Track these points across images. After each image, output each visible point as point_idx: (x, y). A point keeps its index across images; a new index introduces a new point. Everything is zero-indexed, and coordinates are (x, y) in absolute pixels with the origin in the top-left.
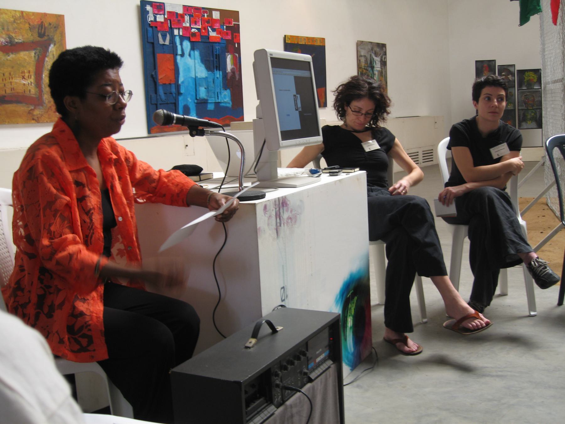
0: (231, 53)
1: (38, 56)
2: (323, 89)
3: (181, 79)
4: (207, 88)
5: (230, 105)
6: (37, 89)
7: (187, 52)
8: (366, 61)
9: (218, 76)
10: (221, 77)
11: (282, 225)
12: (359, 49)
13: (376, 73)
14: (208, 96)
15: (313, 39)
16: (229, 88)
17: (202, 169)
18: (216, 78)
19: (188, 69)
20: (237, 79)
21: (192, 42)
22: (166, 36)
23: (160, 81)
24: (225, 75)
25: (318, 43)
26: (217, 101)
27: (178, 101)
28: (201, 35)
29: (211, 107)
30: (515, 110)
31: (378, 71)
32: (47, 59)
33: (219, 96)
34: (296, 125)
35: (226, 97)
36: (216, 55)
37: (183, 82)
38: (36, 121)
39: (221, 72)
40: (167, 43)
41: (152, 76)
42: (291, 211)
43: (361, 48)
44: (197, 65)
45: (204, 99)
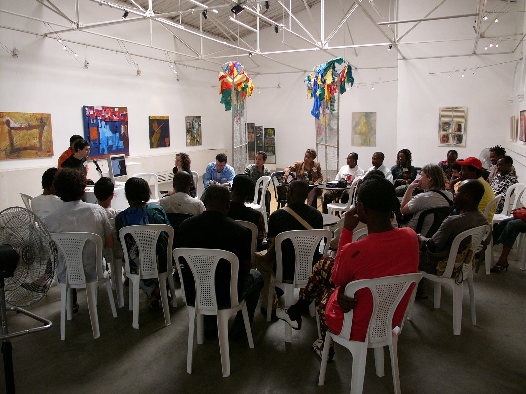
1: (40, 130)
2: (168, 138)
3: (101, 138)
4: (112, 141)
5: (123, 147)
6: (40, 144)
7: (103, 126)
9: (117, 135)
10: (119, 136)
12: (187, 120)
14: (113, 144)
15: (163, 117)
16: (123, 140)
18: (116, 137)
19: (104, 133)
20: (126, 136)
21: (105, 122)
22: (94, 119)
23: (91, 139)
24: (121, 135)
25: (166, 118)
26: (117, 146)
27: (99, 147)
28: (109, 119)
29: (114, 149)
30: (263, 146)
32: (43, 132)
33: (118, 144)
34: (119, 172)
35: (121, 144)
37: (101, 139)
39: (119, 134)
40: (95, 123)
41: (88, 137)
44: (108, 132)
45: (111, 145)
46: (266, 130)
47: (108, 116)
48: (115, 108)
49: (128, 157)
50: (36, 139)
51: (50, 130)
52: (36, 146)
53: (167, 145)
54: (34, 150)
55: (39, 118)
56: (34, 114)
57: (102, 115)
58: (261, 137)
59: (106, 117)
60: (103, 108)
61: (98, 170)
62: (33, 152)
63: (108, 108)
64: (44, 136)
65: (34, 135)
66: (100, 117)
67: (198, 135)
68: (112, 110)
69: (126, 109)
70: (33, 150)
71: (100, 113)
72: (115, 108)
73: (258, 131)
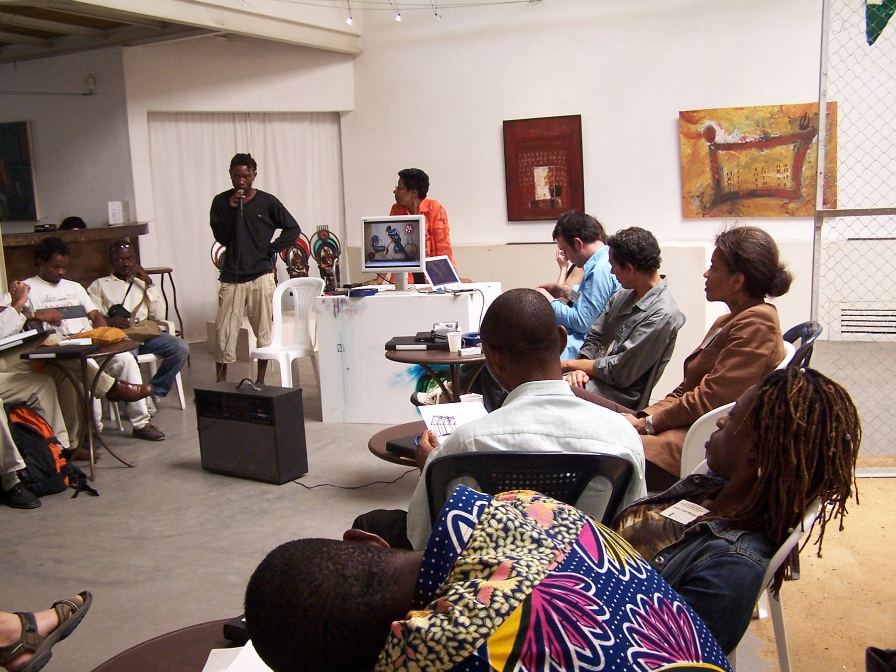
1: (798, 148)
11: (341, 312)
32: (809, 151)
38: (790, 214)
42: (351, 307)
50: (786, 171)
51: (832, 146)
52: (782, 186)
54: (777, 198)
55: (797, 115)
56: (781, 106)
62: (774, 202)
64: (810, 162)
65: (779, 160)
70: (774, 198)
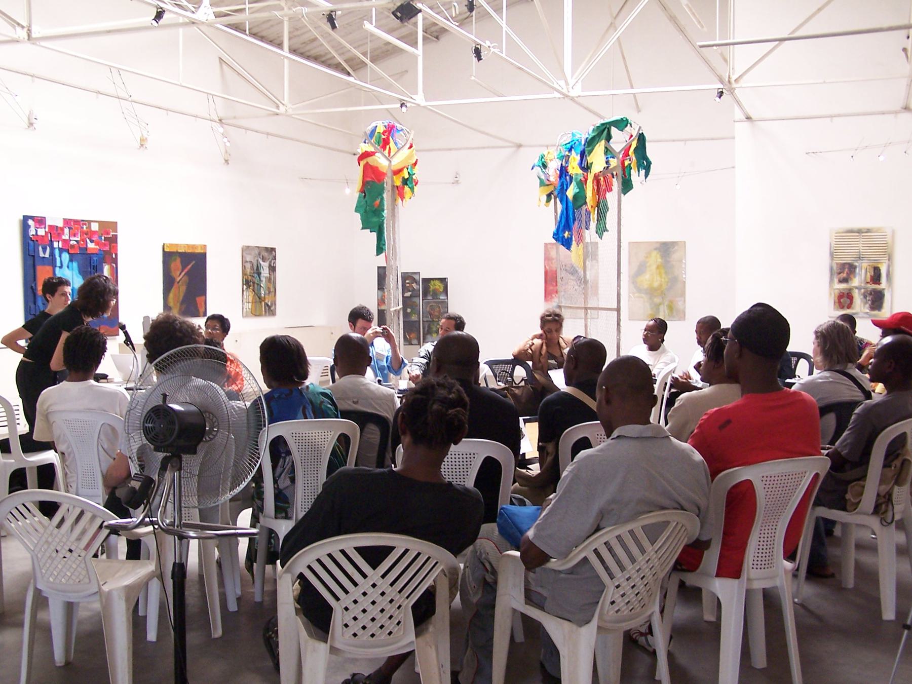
0: (110, 263)
7: (65, 265)
8: (252, 267)
12: (244, 254)
13: (263, 279)
15: (193, 246)
17: (108, 376)
25: (199, 251)
31: (266, 278)
36: (94, 266)
43: (246, 254)
46: (427, 281)
47: (76, 241)
48: (92, 224)
49: (115, 339)
53: (202, 314)
57: (64, 237)
58: (415, 300)
59: (72, 243)
60: (67, 222)
61: (127, 345)
63: (77, 222)
66: (59, 242)
67: (269, 292)
68: (85, 227)
69: (114, 225)
71: (59, 234)
72: (92, 224)
73: (408, 285)
